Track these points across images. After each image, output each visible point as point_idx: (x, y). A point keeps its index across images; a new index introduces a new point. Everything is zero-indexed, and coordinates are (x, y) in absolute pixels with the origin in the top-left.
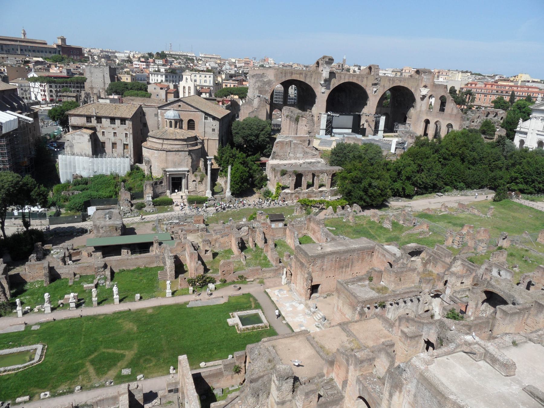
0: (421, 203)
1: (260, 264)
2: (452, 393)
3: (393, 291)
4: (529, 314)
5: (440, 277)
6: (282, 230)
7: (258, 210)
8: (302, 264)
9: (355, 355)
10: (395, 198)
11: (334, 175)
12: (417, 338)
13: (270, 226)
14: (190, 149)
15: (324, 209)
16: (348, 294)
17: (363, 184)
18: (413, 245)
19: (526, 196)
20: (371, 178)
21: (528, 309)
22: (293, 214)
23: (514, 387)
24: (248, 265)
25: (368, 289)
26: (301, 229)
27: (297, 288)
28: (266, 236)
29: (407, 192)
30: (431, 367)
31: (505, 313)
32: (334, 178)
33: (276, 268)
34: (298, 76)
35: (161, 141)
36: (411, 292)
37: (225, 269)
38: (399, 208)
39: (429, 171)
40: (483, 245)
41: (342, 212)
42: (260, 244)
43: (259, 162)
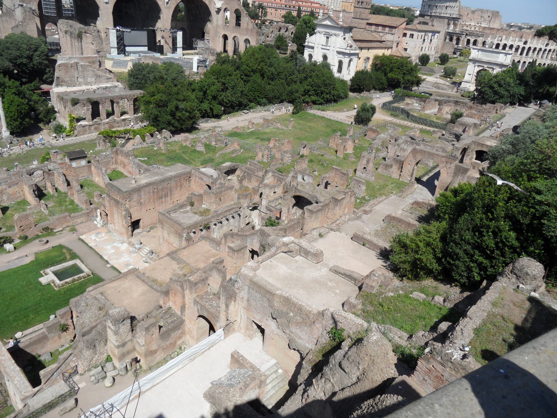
1: (67, 210)
3: (216, 212)
4: (329, 208)
5: (255, 191)
6: (87, 168)
7: (51, 149)
8: (117, 202)
9: (188, 280)
11: (136, 100)
12: (243, 250)
13: (70, 166)
15: (131, 139)
16: (172, 222)
17: (169, 107)
18: (227, 165)
19: (317, 106)
20: (177, 100)
21: (327, 205)
22: (96, 149)
23: (323, 270)
25: (190, 214)
26: (109, 164)
27: (117, 228)
28: (68, 178)
29: (215, 112)
30: (258, 272)
31: (311, 212)
32: (137, 103)
33: (88, 211)
36: (231, 209)
37: (23, 223)
38: (210, 130)
39: (233, 89)
40: (288, 155)
41: (152, 140)
42: (63, 187)
43: (39, 91)
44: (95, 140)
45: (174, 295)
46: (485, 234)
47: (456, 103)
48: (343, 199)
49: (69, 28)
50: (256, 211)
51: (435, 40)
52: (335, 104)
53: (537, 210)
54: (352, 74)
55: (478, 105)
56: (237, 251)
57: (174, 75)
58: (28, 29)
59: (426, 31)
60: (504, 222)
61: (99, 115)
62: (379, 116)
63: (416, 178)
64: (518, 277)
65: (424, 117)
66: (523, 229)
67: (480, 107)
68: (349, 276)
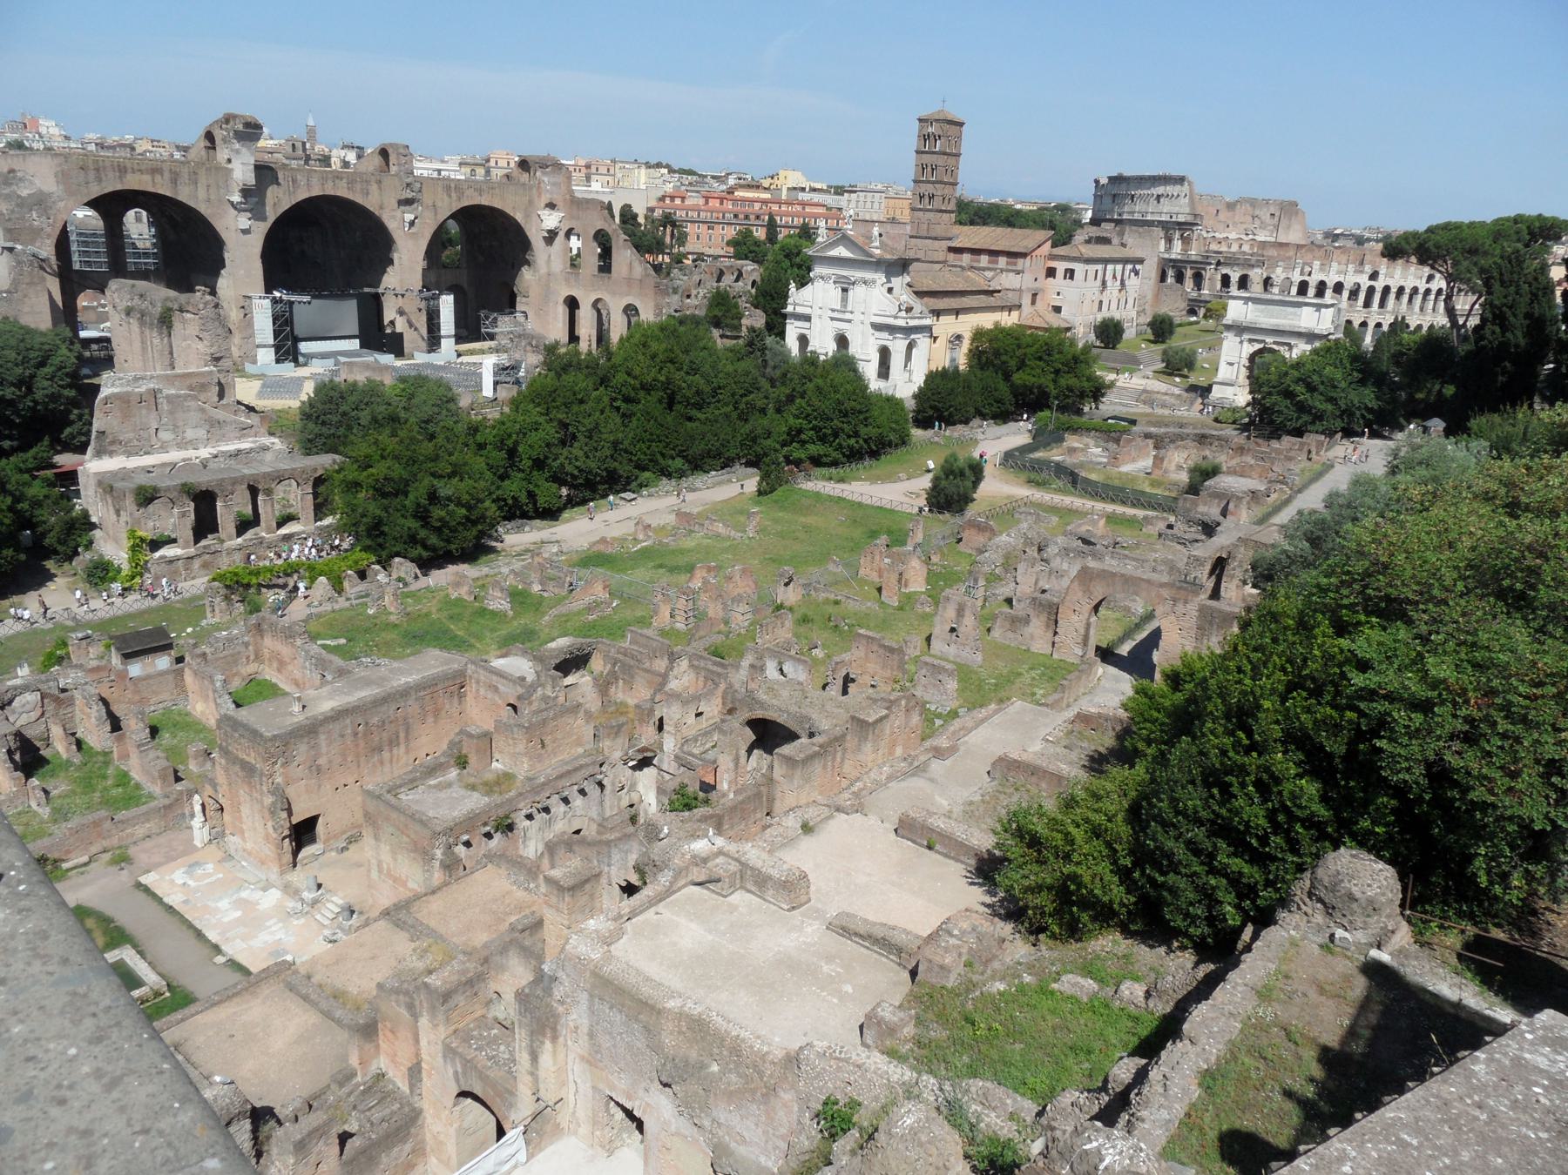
0: (579, 530)
1: (107, 802)
2: (673, 994)
3: (530, 779)
4: (845, 750)
5: (644, 712)
6: (170, 677)
7: (73, 630)
8: (249, 770)
9: (426, 985)
10: (513, 524)
11: (318, 482)
12: (588, 887)
13: (123, 675)
17: (411, 496)
18: (561, 644)
19: (824, 471)
20: (434, 475)
21: (839, 740)
23: (809, 930)
24: (60, 815)
25: (457, 792)
26: (236, 662)
27: (249, 846)
28: (114, 708)
29: (542, 502)
30: (618, 949)
31: (790, 761)
32: (321, 489)
33: (167, 802)
34: (147, 177)
36: (576, 770)
38: (527, 551)
39: (590, 438)
40: (743, 608)
41: (362, 587)
44: (200, 597)
45: (389, 1034)
46: (1235, 789)
47: (1202, 439)
48: (881, 719)
49: (137, 301)
50: (649, 772)
51: (1133, 282)
52: (874, 463)
53: (1362, 714)
54: (919, 380)
55: (1260, 441)
56: (572, 889)
57: (429, 410)
58: (26, 309)
59: (1106, 261)
60: (1285, 752)
61: (215, 529)
62: (995, 487)
63: (1098, 648)
64: (1329, 909)
65: (1117, 483)
66: (1336, 771)
67: (1264, 447)
68: (882, 942)
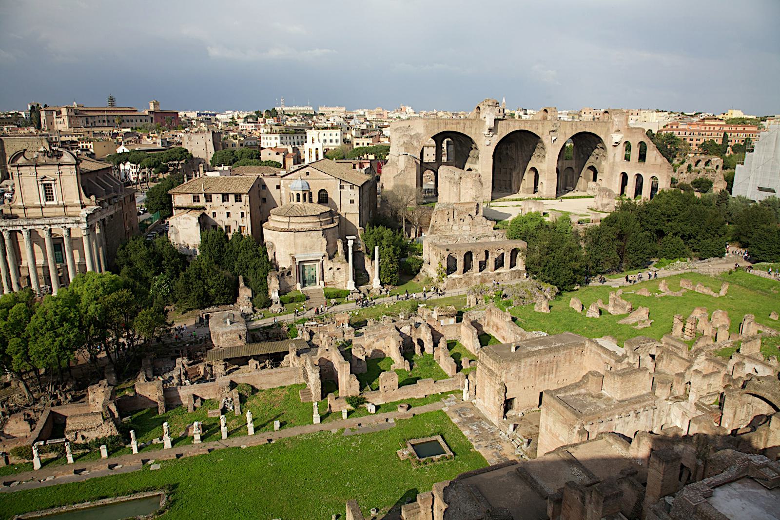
8: (491, 372)
14: (324, 227)
27: (486, 405)
34: (454, 126)
35: (287, 219)
